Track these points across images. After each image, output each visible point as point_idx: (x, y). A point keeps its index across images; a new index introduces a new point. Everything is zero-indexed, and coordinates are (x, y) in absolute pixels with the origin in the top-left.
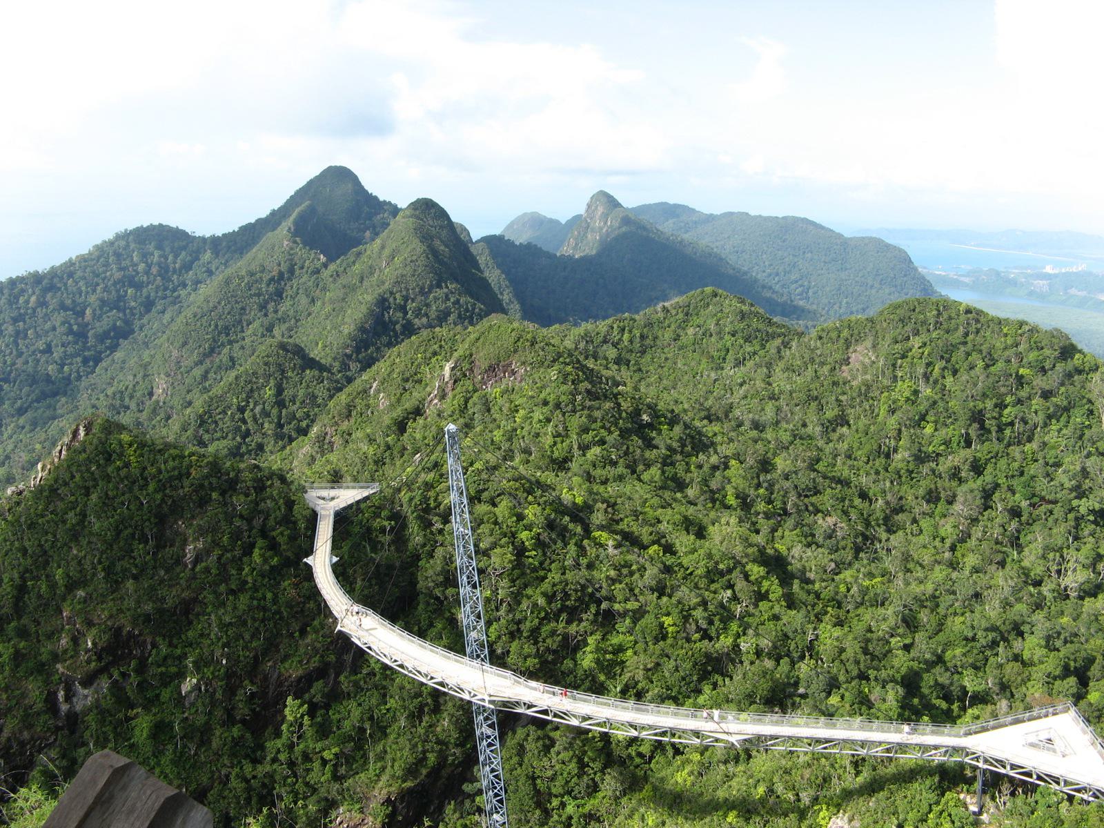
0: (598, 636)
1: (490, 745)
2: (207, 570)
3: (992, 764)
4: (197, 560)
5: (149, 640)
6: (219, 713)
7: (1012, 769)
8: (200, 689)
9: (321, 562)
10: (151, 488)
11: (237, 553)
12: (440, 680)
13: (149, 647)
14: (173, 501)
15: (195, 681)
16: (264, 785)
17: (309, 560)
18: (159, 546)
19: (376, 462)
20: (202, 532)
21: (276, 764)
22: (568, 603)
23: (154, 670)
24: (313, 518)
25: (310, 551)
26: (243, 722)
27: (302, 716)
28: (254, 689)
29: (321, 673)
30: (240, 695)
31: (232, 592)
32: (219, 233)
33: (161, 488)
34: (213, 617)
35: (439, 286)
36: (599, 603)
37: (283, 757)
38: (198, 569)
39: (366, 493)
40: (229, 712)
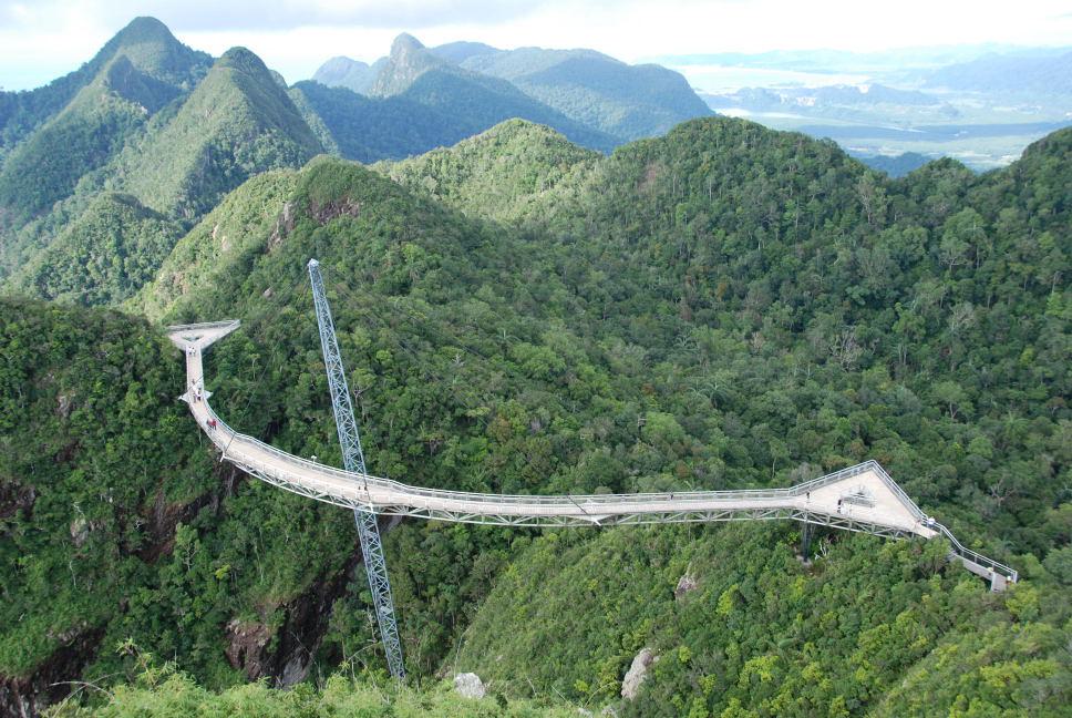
0: (456, 438)
1: (373, 546)
2: (83, 417)
3: (814, 519)
4: (71, 410)
5: (32, 490)
6: (112, 548)
7: (831, 521)
8: (90, 529)
9: (197, 397)
10: (14, 344)
11: (112, 396)
12: (325, 494)
13: (33, 495)
14: (40, 355)
15: (83, 522)
16: (164, 608)
17: (184, 398)
18: (31, 400)
19: (228, 300)
20: (73, 382)
21: (171, 587)
22: (426, 413)
23: (37, 518)
24: (182, 360)
25: (183, 389)
26: (136, 553)
27: (192, 542)
28: (143, 521)
29: (205, 500)
30: (130, 528)
31: (111, 434)
32: (30, 88)
33: (26, 342)
34: (94, 460)
35: (262, 132)
36: (452, 409)
37: (178, 581)
38: (74, 415)
39: (227, 330)
40: (122, 546)
